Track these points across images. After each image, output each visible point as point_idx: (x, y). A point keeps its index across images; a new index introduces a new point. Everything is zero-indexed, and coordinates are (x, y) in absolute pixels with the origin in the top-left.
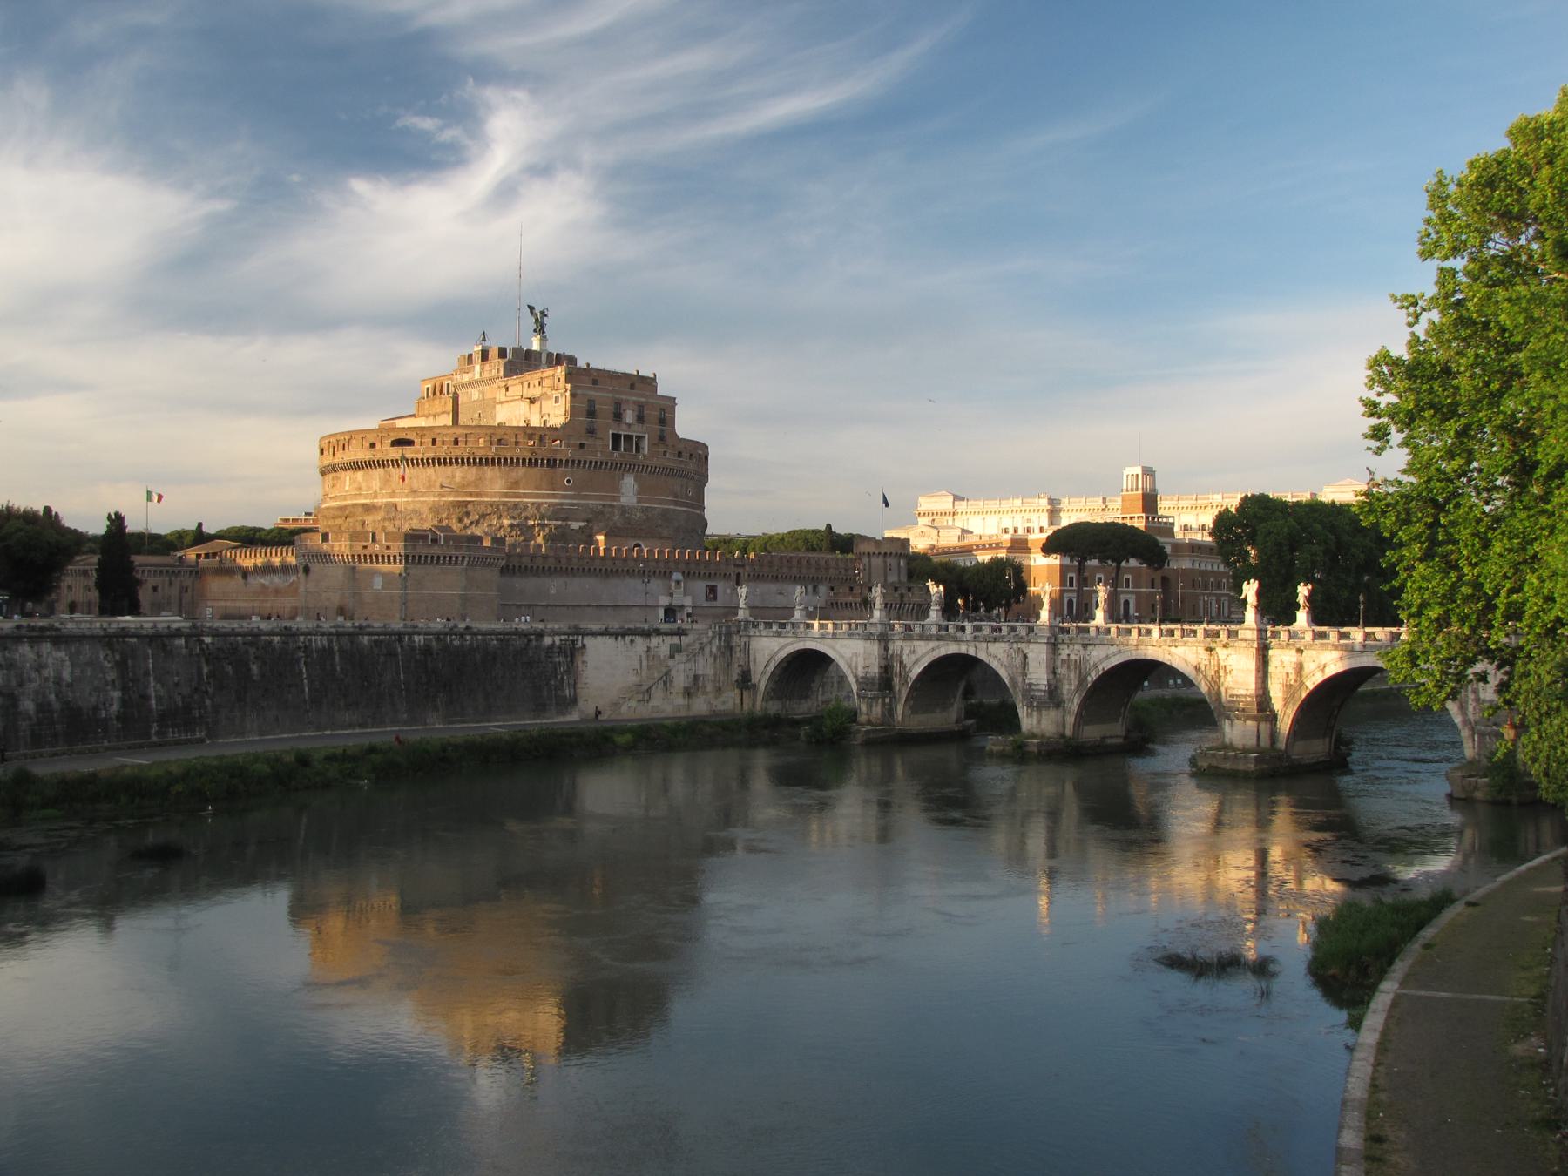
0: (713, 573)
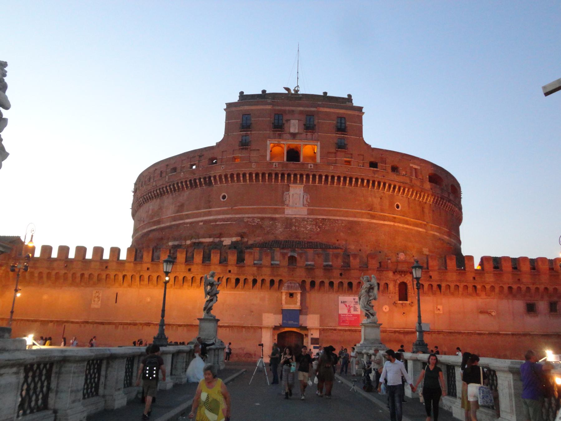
0: (355, 283)
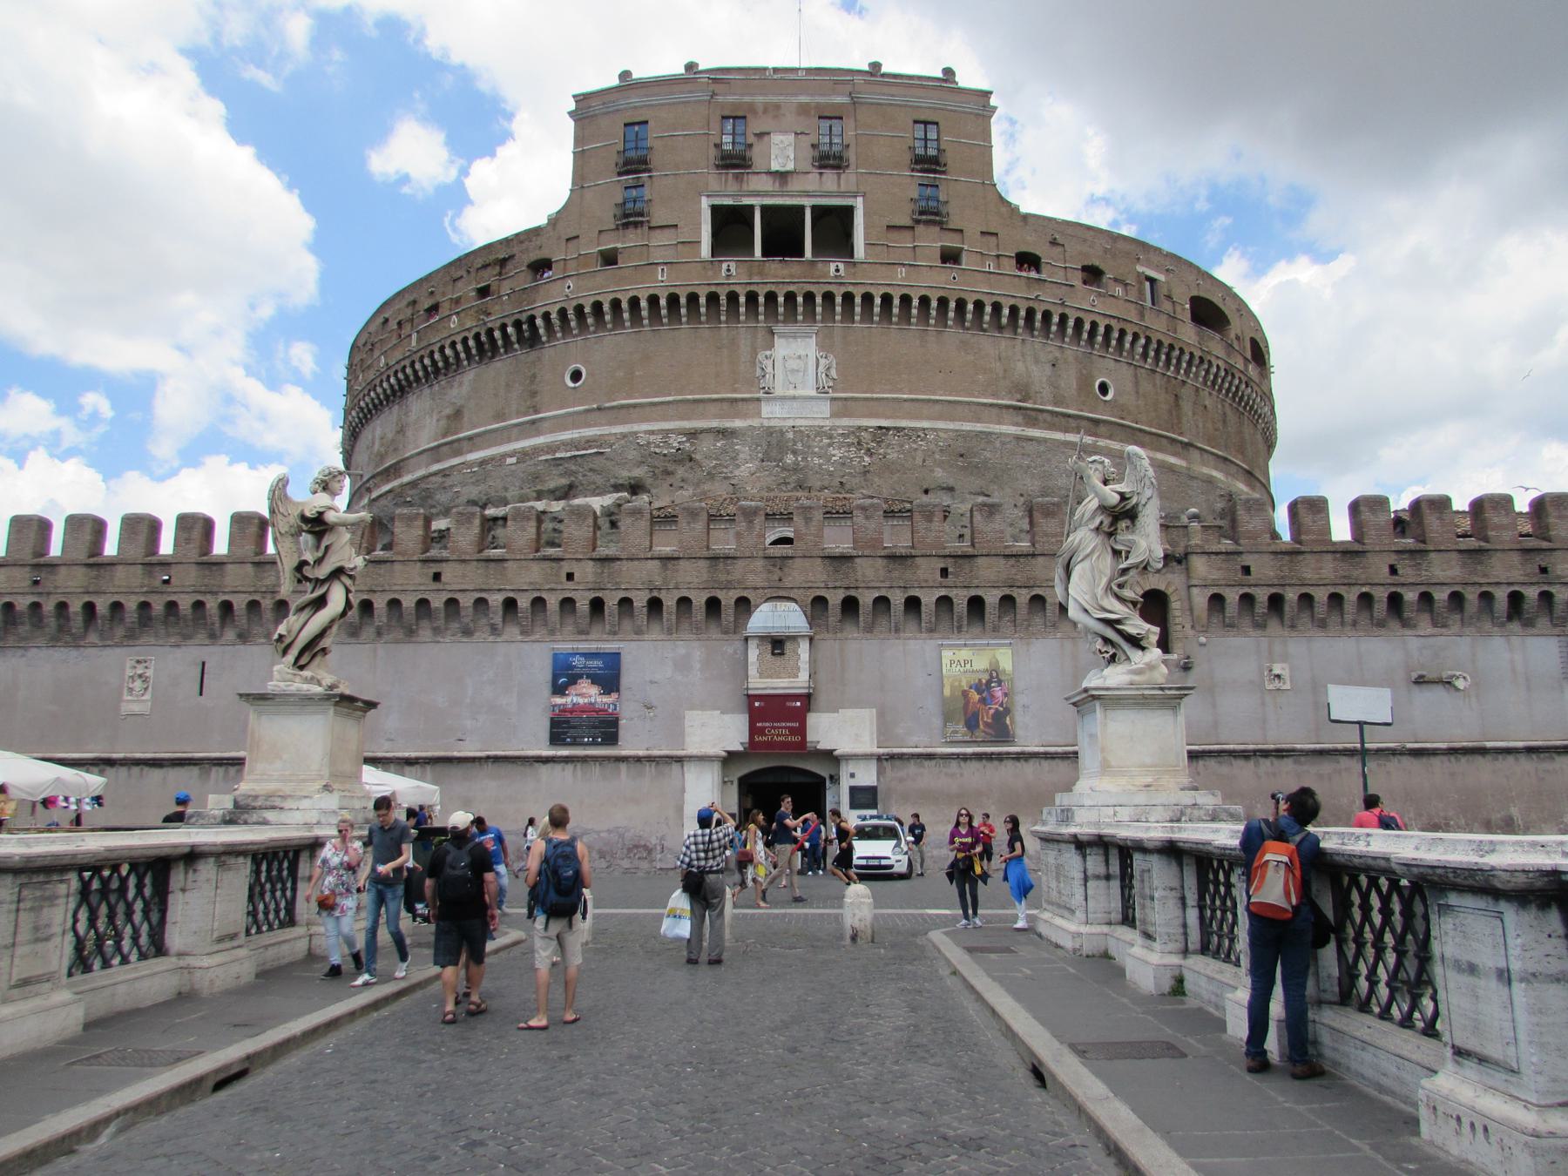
0: (992, 598)
